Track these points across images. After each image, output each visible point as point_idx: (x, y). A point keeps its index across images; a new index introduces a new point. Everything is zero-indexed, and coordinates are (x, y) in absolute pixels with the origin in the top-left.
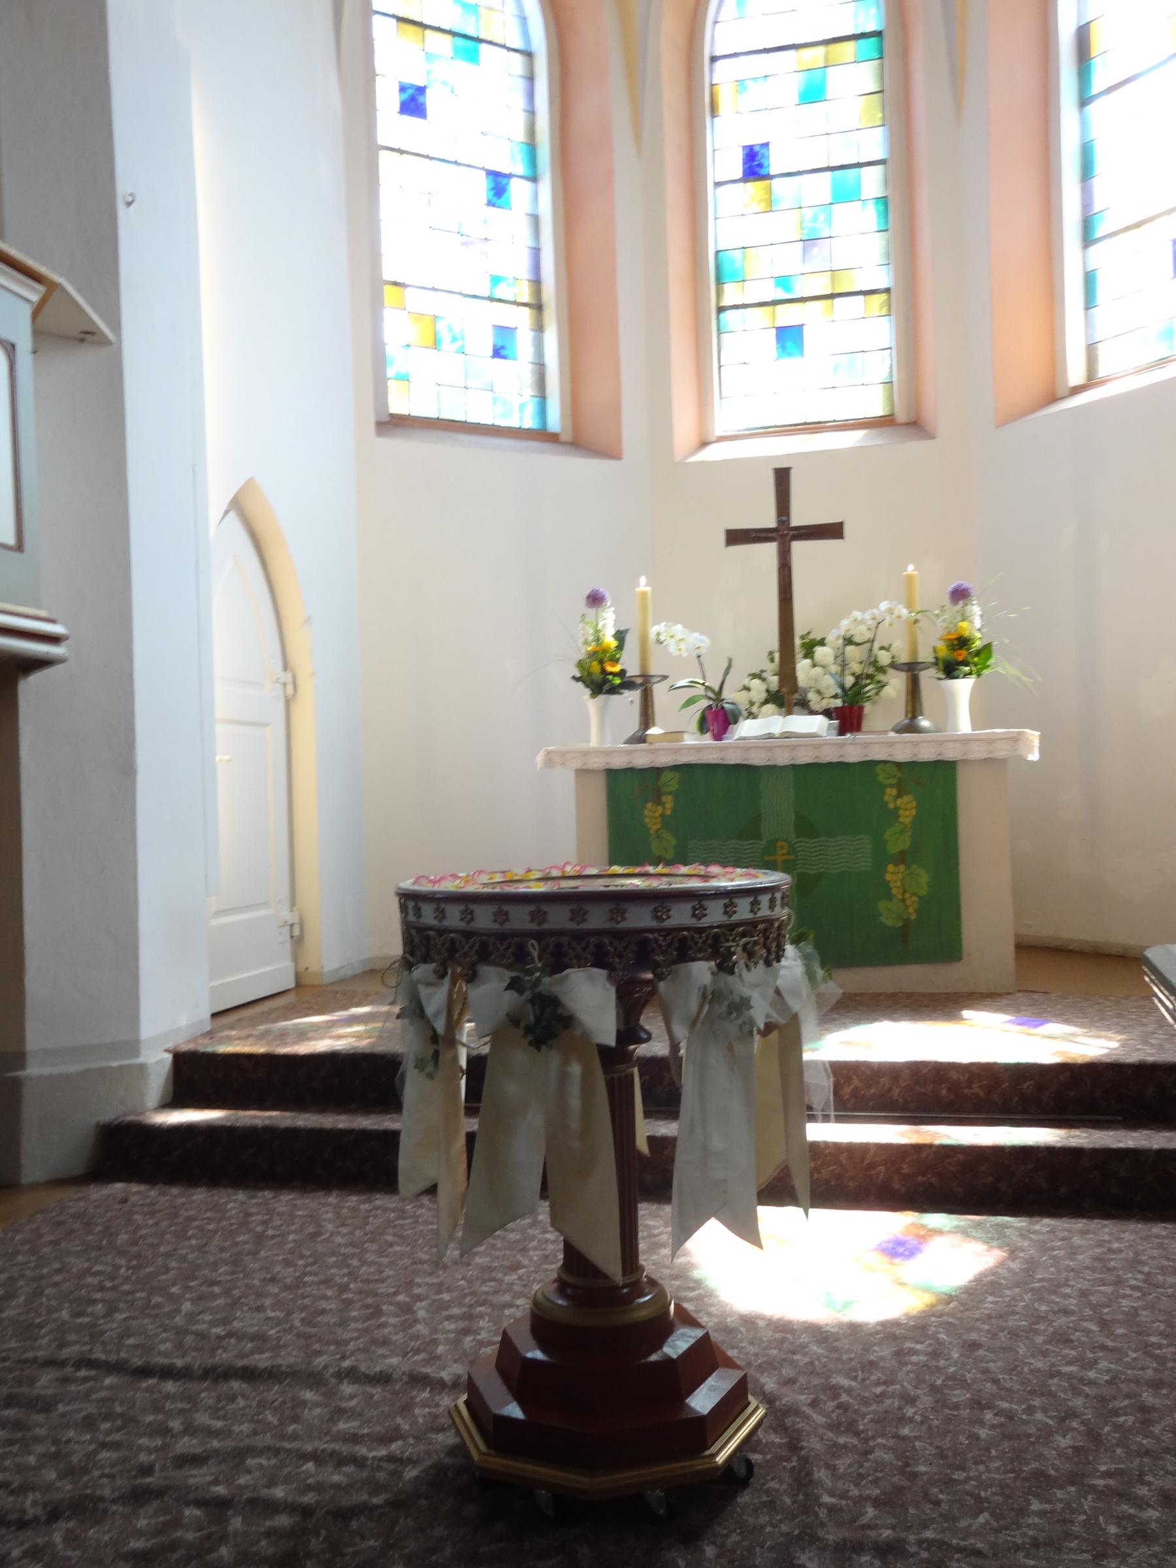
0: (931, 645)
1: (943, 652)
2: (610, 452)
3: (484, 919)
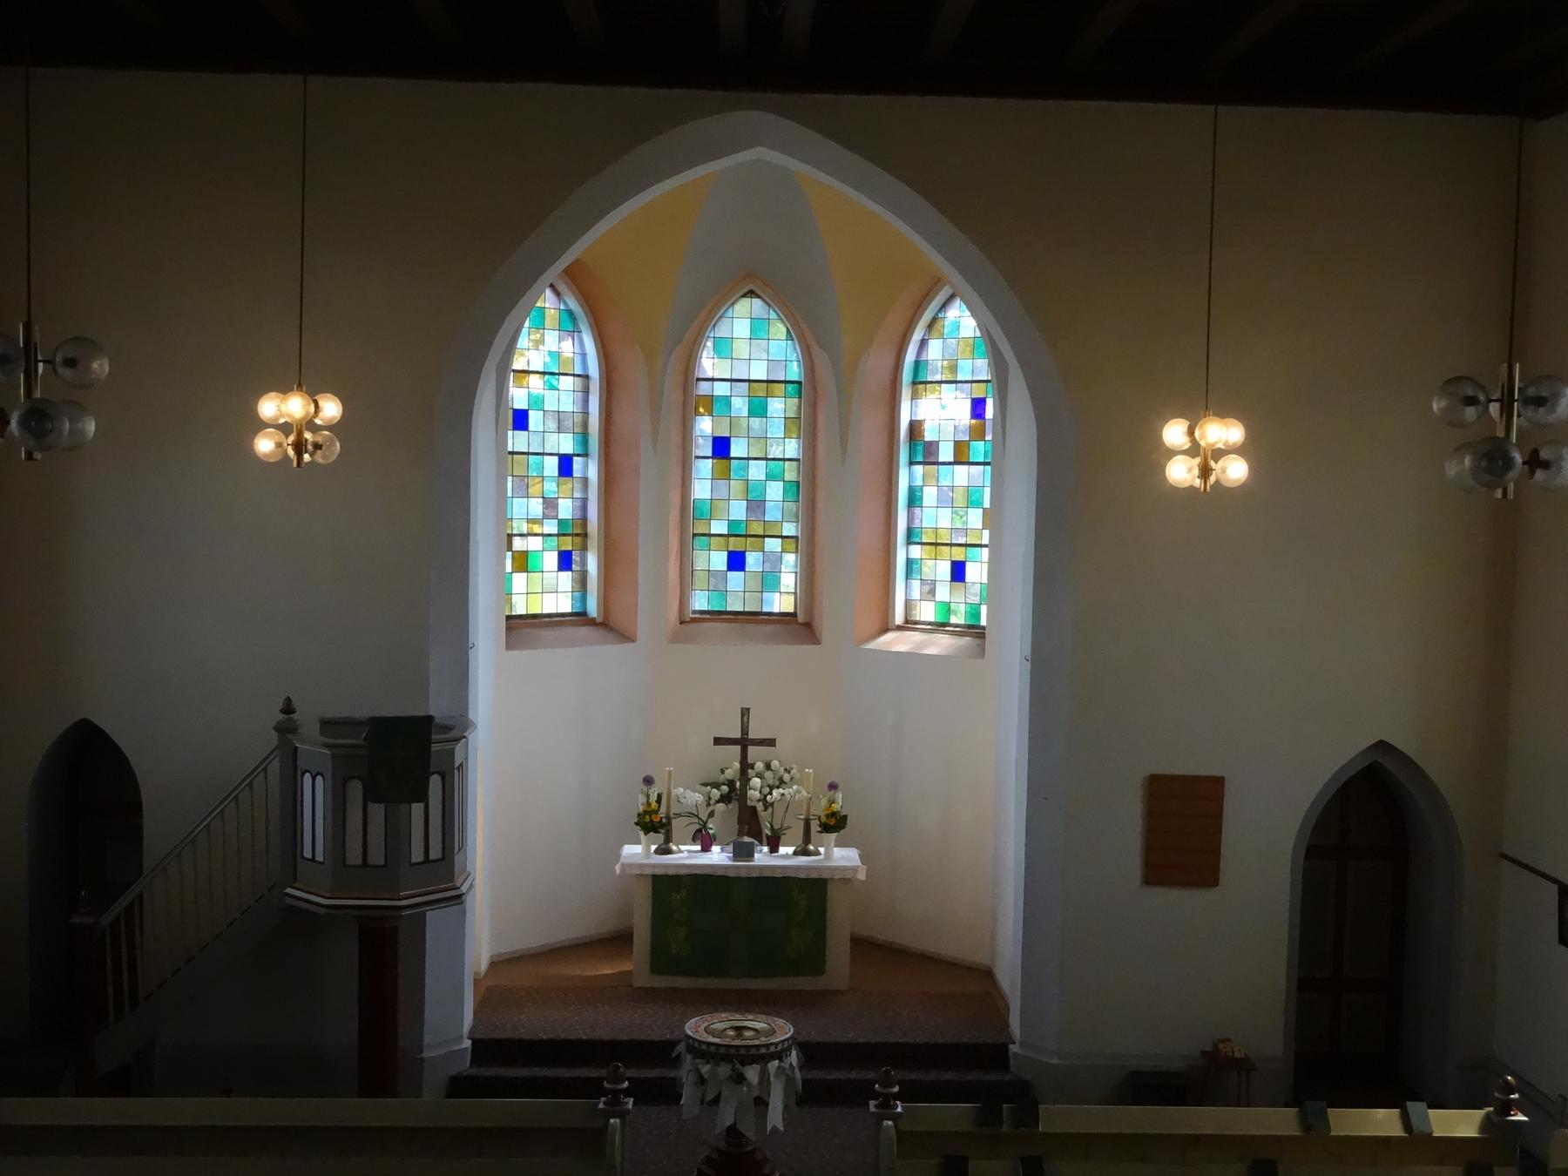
0: (820, 808)
1: (824, 819)
2: (626, 637)
3: (722, 1050)
